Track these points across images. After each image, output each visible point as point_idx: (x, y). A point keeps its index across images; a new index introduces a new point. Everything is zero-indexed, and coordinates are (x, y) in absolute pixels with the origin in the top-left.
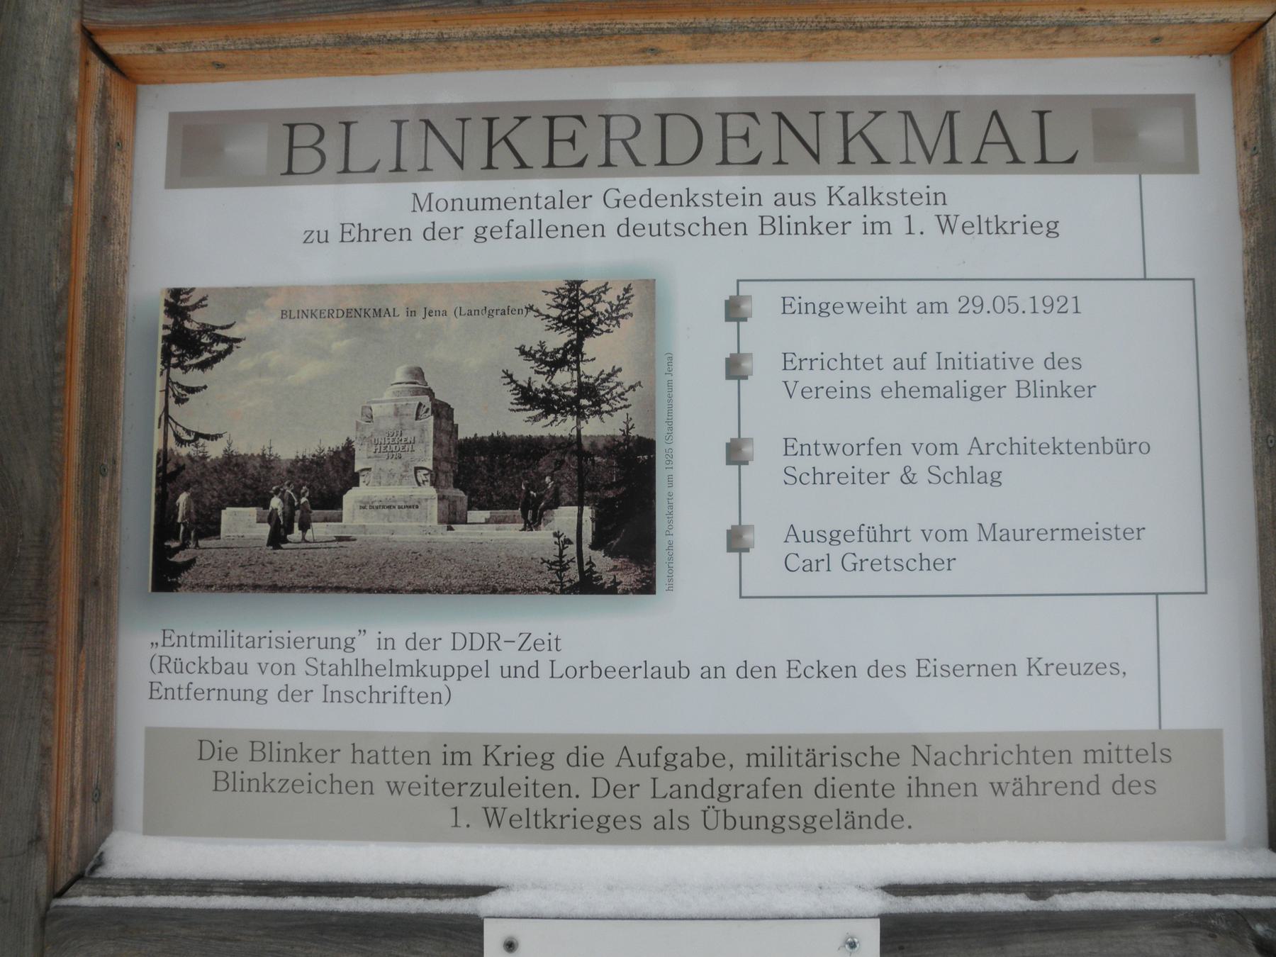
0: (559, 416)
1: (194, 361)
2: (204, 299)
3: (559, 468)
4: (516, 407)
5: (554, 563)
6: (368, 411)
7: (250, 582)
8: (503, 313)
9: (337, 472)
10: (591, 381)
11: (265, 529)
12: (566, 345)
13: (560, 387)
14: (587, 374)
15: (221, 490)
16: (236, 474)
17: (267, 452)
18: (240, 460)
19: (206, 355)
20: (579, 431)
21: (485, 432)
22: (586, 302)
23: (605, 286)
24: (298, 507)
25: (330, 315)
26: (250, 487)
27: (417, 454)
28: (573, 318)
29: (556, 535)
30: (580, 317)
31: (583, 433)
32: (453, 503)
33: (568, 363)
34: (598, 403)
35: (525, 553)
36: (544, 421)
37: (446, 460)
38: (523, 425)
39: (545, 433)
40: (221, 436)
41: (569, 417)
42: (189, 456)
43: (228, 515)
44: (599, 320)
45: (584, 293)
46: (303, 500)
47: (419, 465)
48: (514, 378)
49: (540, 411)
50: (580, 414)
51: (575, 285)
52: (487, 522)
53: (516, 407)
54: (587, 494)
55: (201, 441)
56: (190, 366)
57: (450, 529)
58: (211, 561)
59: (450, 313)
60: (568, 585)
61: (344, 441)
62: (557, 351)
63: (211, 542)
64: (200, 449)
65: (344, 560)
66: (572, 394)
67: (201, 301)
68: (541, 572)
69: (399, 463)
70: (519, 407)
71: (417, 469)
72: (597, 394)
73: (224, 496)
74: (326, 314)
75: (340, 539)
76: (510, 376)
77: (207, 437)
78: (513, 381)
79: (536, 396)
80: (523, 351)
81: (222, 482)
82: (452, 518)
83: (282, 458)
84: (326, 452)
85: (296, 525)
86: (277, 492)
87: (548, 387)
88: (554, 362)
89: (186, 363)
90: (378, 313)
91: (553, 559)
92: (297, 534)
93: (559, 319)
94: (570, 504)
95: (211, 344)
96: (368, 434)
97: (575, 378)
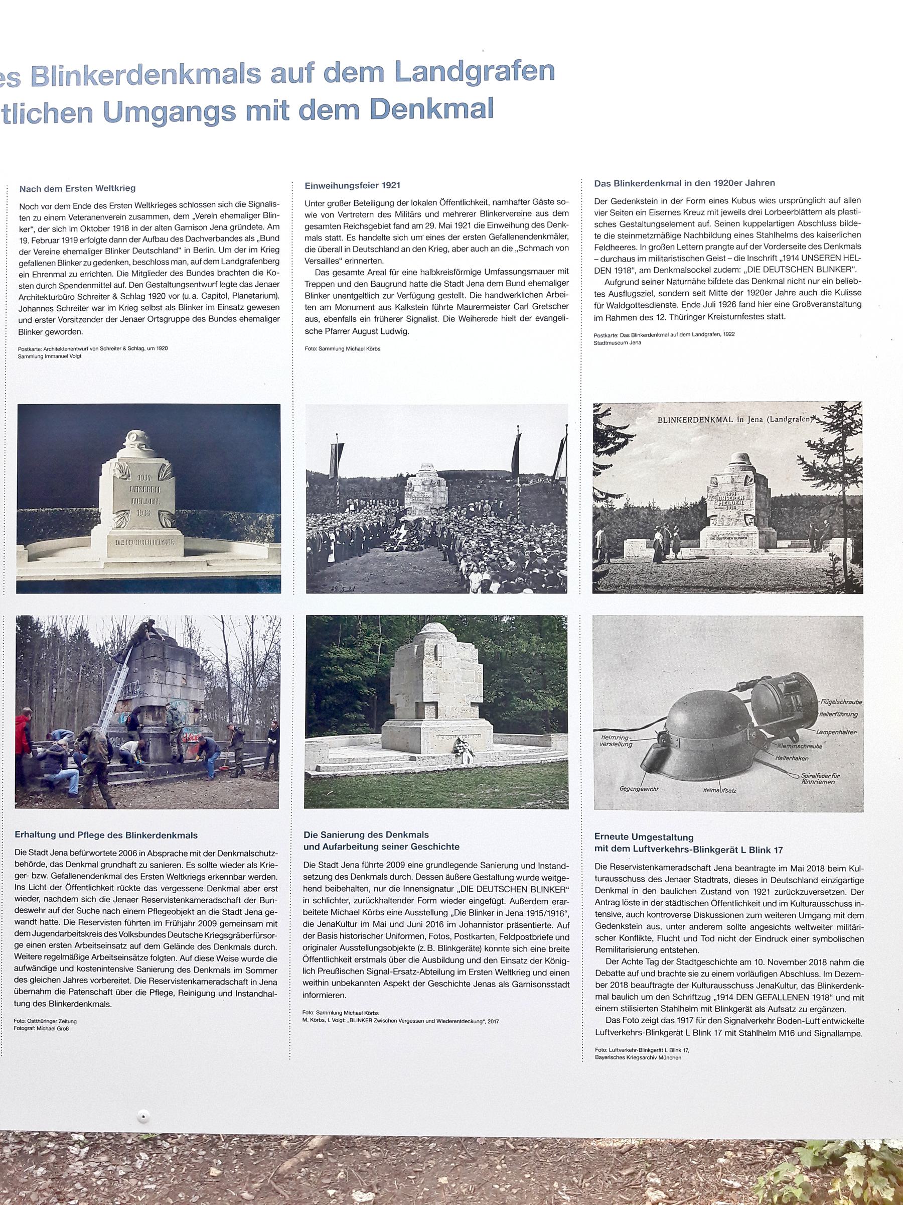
0: (832, 484)
1: (604, 449)
2: (609, 410)
3: (832, 515)
4: (806, 478)
5: (829, 572)
6: (714, 480)
7: (643, 583)
8: (797, 421)
9: (696, 517)
10: (851, 462)
11: (651, 552)
12: (836, 440)
13: (832, 466)
14: (849, 458)
15: (623, 529)
16: (632, 518)
17: (652, 505)
18: (635, 510)
19: (611, 446)
20: (844, 493)
21: (787, 493)
22: (848, 414)
23: (859, 404)
24: (672, 539)
25: (689, 421)
26: (642, 527)
27: (745, 507)
28: (840, 424)
29: (831, 555)
30: (844, 423)
31: (846, 494)
32: (768, 535)
33: (837, 452)
34: (855, 476)
35: (812, 566)
36: (823, 487)
37: (764, 510)
38: (809, 489)
39: (824, 494)
40: (622, 495)
41: (838, 485)
42: (602, 507)
43: (628, 543)
44: (856, 425)
45: (846, 408)
46: (675, 534)
47: (747, 513)
48: (805, 460)
49: (821, 480)
50: (845, 483)
51: (840, 404)
52: (789, 547)
53: (806, 478)
54: (849, 530)
55: (610, 499)
56: (602, 452)
57: (767, 551)
58: (619, 571)
59: (765, 420)
60: (838, 584)
61: (700, 499)
62: (830, 444)
63: (619, 560)
64: (610, 503)
65: (701, 570)
66: (839, 470)
67: (607, 411)
68: (822, 577)
69: (735, 512)
70: (808, 478)
71: (746, 516)
72: (855, 471)
73: (626, 532)
74: (687, 420)
75: (698, 557)
76: (802, 459)
77: (613, 496)
78: (804, 462)
79: (818, 471)
80: (809, 443)
81: (624, 524)
82: (767, 545)
83: (530, 591)
84: (689, 505)
85: (671, 549)
86: (658, 530)
87: (825, 466)
88: (827, 451)
89: (599, 450)
90: (719, 420)
91: (829, 569)
92: (671, 555)
93: (831, 424)
94: (839, 537)
95: (614, 439)
96: (715, 495)
97: (842, 461)
